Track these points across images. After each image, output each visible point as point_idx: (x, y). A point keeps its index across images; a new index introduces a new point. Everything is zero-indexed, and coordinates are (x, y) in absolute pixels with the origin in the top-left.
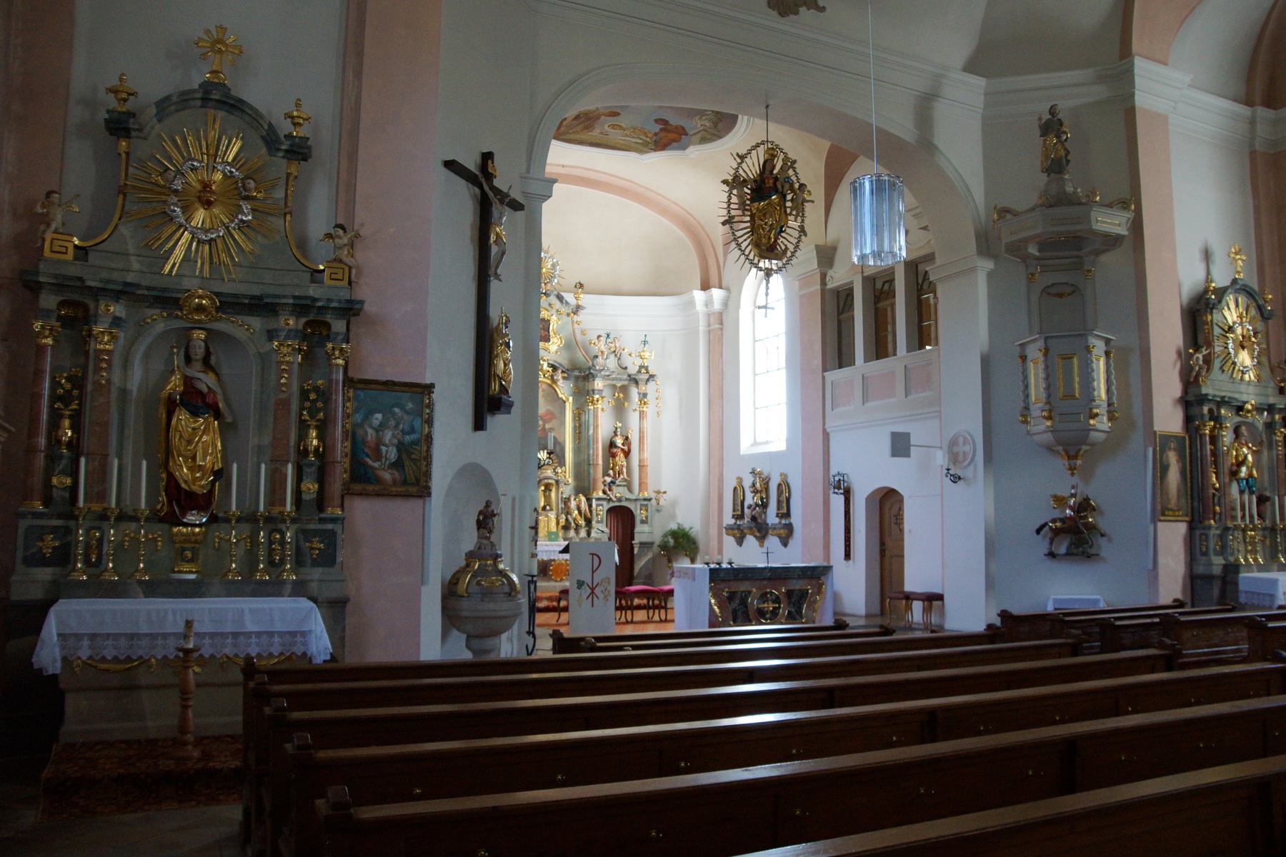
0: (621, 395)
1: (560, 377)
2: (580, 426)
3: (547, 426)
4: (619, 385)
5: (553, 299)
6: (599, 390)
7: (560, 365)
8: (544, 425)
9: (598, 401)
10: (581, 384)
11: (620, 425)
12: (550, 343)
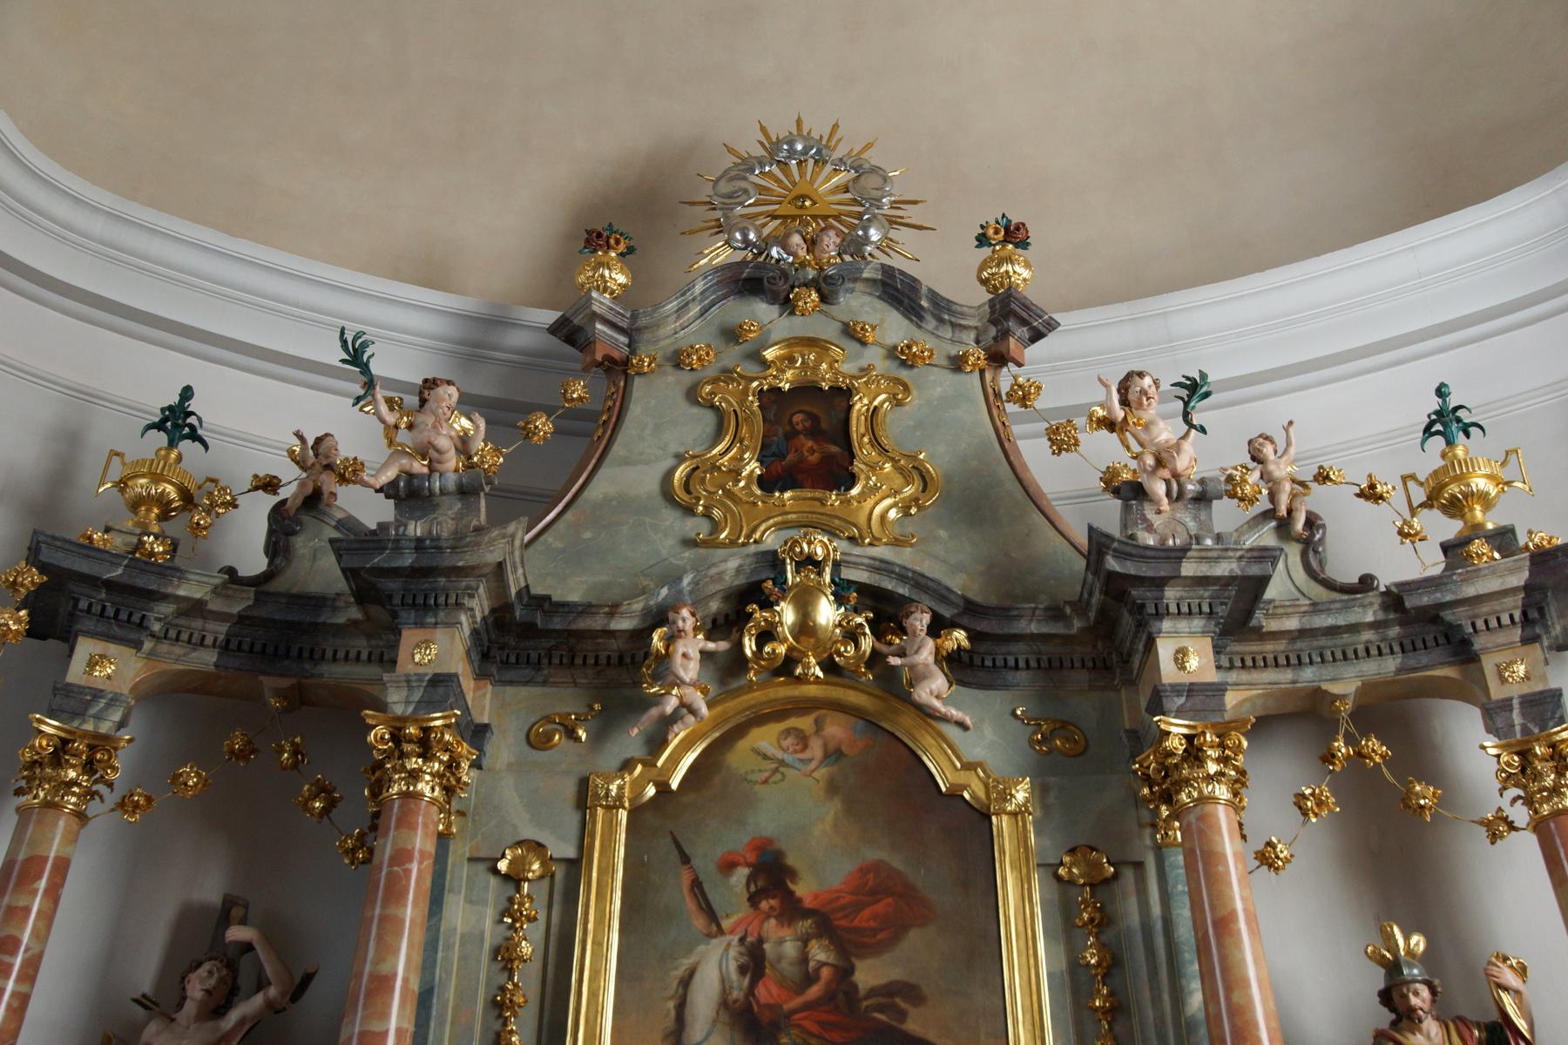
0: (1375, 747)
1: (926, 654)
2: (1113, 964)
3: (868, 974)
4: (1345, 683)
5: (859, 304)
6: (1192, 690)
7: (920, 582)
8: (844, 973)
9: (1194, 753)
10: (1084, 706)
11: (1418, 942)
12: (855, 491)
